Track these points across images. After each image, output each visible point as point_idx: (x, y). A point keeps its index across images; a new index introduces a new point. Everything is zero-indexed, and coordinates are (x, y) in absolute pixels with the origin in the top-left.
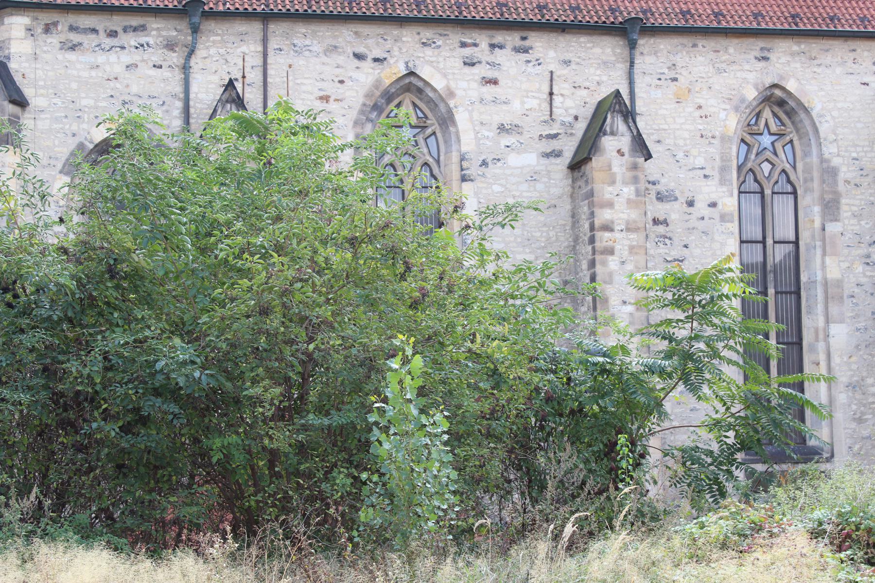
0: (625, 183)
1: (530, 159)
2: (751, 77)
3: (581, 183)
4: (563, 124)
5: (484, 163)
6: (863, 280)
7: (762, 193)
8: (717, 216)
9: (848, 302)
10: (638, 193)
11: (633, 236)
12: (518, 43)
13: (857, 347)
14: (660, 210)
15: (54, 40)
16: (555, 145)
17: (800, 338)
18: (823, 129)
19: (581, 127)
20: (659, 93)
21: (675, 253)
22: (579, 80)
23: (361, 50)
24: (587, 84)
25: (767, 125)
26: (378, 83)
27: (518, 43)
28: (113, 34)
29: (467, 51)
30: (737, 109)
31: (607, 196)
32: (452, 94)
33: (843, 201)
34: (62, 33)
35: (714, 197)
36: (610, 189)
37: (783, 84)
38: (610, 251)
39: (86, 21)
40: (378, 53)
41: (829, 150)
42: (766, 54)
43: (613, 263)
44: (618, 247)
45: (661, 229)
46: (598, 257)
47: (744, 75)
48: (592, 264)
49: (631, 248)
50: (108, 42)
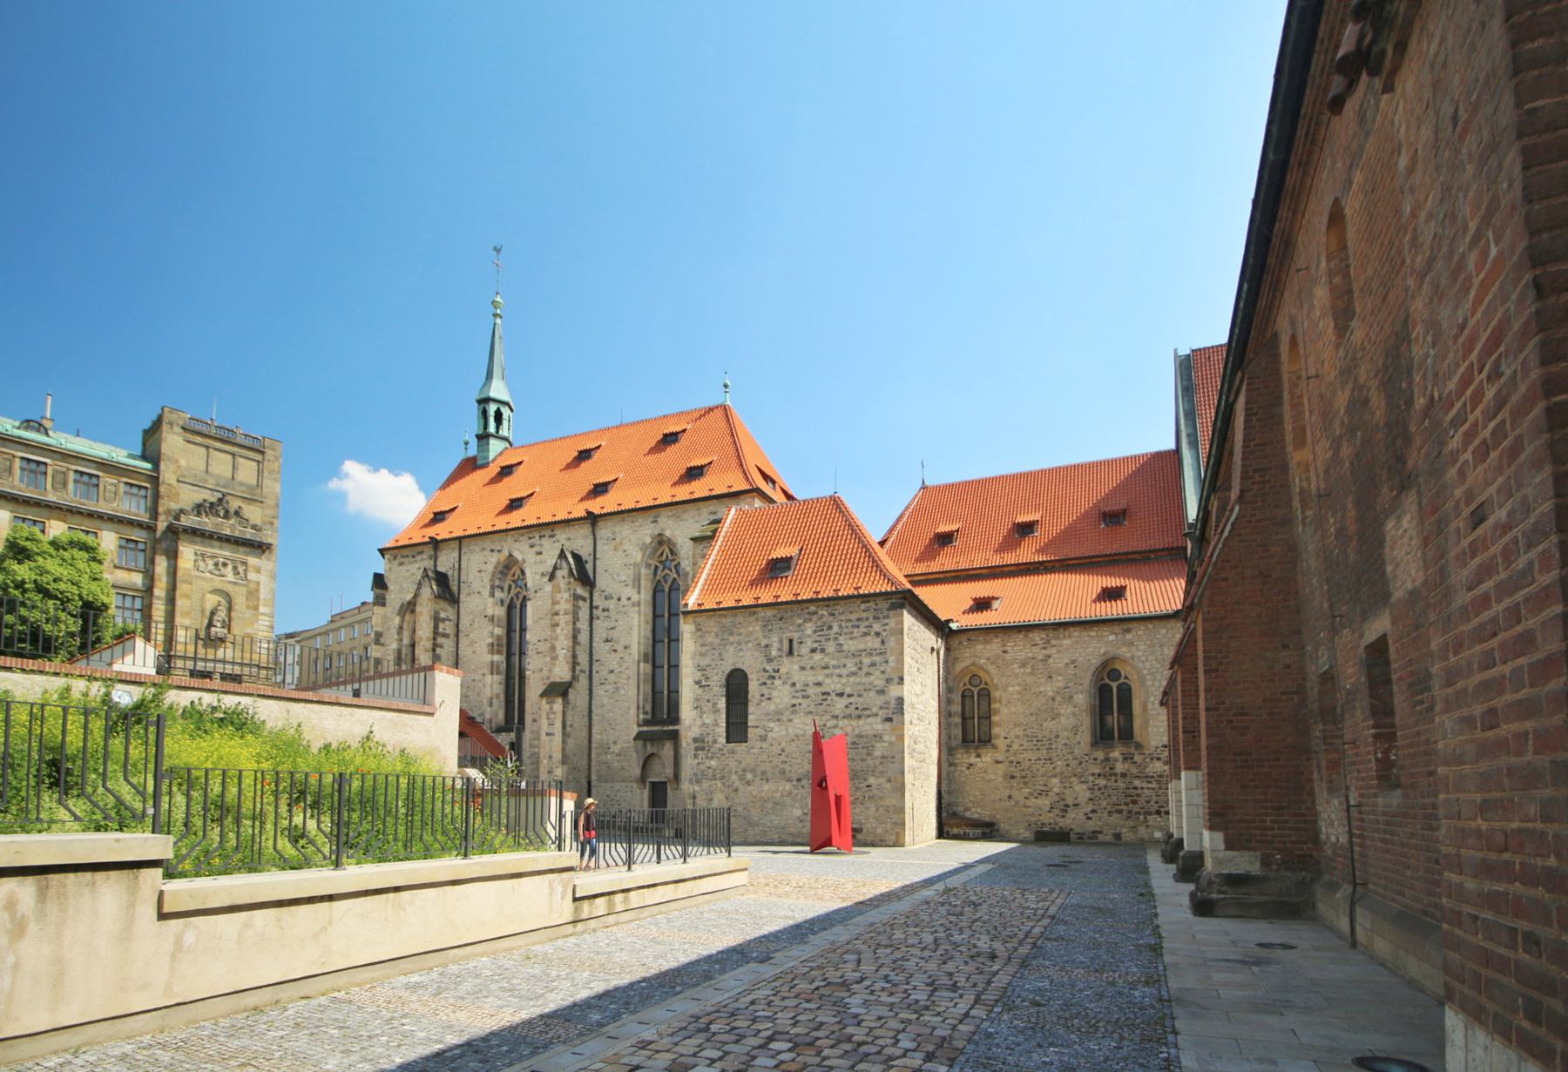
2: (649, 532)
5: (536, 591)
15: (396, 562)
21: (612, 625)
23: (493, 547)
26: (498, 562)
28: (414, 556)
30: (641, 549)
32: (524, 561)
34: (400, 560)
35: (629, 595)
38: (557, 625)
39: (405, 552)
40: (499, 548)
43: (558, 630)
45: (606, 614)
50: (412, 559)
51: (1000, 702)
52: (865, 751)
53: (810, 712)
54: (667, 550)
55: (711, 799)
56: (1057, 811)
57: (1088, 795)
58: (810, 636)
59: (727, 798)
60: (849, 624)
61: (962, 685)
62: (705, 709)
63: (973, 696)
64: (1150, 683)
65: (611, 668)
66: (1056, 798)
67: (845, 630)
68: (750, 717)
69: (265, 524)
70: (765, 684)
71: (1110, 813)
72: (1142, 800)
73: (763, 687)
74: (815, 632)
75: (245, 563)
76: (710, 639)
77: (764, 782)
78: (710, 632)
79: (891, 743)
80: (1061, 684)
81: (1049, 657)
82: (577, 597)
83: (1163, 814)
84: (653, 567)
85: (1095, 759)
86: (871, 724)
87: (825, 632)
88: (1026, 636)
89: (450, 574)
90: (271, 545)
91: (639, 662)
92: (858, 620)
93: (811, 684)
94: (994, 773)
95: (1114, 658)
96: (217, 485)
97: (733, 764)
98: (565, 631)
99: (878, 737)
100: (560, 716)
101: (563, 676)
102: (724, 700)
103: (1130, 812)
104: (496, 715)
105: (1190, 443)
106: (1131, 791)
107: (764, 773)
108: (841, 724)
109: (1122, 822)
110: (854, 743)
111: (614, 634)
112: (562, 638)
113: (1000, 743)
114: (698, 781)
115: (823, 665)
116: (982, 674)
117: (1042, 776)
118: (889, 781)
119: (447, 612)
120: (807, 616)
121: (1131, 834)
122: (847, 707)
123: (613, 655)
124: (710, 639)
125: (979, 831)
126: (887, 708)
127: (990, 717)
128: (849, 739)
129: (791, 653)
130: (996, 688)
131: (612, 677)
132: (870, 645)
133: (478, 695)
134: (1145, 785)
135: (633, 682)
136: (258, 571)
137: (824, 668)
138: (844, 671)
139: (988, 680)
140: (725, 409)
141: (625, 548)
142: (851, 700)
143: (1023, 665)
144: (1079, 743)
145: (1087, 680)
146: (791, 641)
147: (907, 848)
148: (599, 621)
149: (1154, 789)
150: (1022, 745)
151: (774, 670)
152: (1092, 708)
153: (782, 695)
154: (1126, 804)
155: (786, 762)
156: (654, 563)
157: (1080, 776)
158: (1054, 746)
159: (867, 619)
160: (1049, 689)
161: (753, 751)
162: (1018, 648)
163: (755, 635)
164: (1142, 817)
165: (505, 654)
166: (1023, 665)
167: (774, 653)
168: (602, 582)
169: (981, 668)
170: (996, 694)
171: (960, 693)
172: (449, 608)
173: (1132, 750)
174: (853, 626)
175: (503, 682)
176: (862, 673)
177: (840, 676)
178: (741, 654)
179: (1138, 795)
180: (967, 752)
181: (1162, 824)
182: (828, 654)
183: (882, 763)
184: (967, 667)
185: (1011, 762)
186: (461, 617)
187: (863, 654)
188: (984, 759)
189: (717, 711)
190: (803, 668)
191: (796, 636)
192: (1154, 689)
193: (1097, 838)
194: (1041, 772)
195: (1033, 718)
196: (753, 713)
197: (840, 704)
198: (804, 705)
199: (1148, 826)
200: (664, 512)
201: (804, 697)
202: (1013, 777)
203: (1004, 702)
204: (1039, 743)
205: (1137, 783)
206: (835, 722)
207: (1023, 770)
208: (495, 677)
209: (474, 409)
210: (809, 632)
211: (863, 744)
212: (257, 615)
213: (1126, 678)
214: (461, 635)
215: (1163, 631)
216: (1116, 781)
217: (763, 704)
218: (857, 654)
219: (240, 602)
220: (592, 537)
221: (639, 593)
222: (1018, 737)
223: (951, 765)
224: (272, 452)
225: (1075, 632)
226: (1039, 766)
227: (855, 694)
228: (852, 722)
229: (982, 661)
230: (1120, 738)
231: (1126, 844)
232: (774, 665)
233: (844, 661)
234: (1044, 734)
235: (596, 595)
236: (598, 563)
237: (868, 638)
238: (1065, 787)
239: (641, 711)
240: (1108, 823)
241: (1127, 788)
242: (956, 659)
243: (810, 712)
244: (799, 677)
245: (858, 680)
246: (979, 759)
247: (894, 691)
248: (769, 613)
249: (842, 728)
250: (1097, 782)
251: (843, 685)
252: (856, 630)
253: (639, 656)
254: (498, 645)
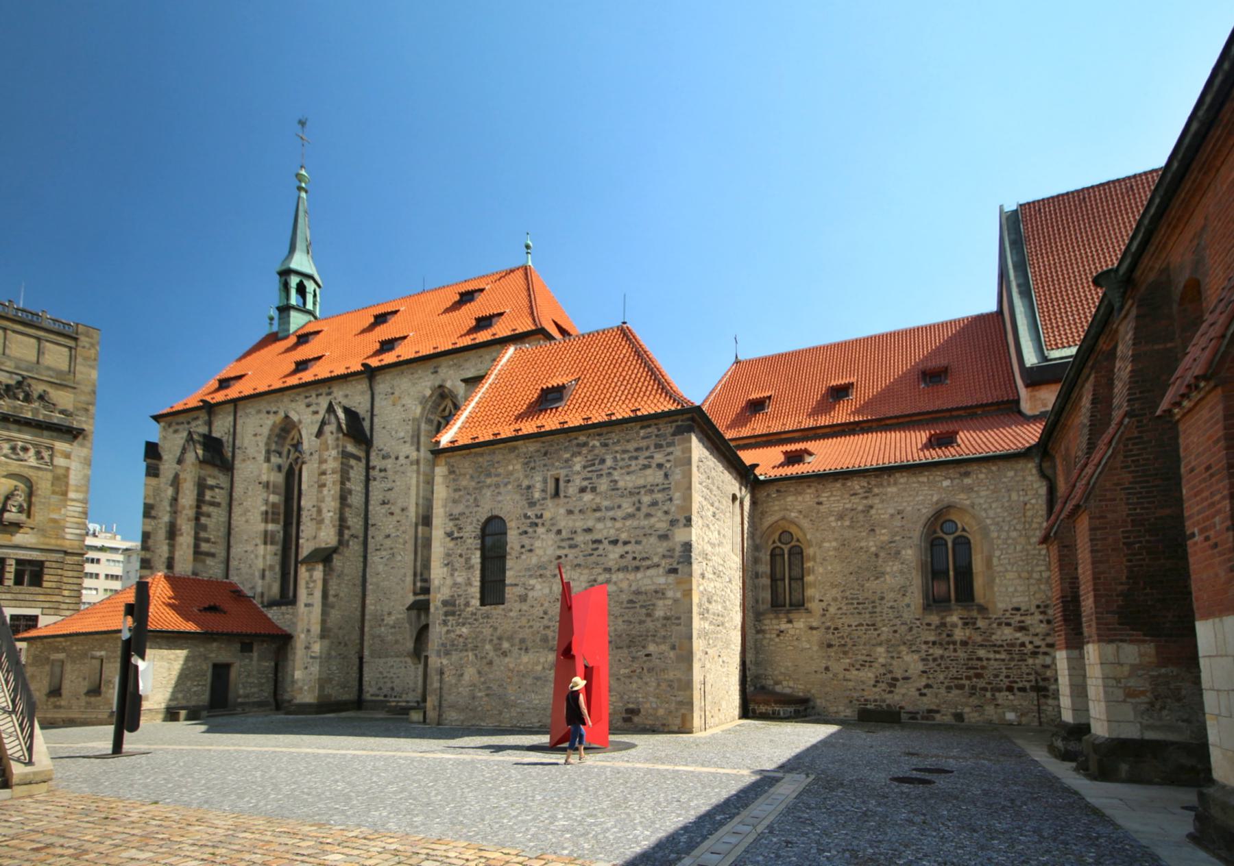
0: (333, 449)
2: (429, 384)
5: (311, 454)
11: (335, 476)
12: (327, 390)
20: (384, 403)
23: (269, 409)
26: (274, 425)
27: (327, 390)
29: (307, 400)
30: (421, 403)
32: (300, 422)
38: (324, 485)
40: (274, 409)
43: (325, 491)
51: (814, 559)
52: (644, 611)
53: (579, 565)
54: (450, 405)
55: (462, 675)
56: (884, 686)
57: (921, 667)
58: (578, 473)
59: (479, 673)
61: (770, 542)
62: (457, 565)
63: (783, 555)
64: (995, 535)
65: (387, 532)
66: (882, 671)
67: (621, 464)
68: (509, 574)
69: (78, 410)
70: (526, 532)
71: (949, 688)
72: (988, 674)
73: (524, 536)
74: (585, 467)
75: (51, 448)
76: (464, 482)
77: (523, 652)
78: (465, 475)
79: (676, 601)
80: (885, 538)
81: (871, 507)
82: (345, 455)
83: (1016, 690)
84: (435, 423)
85: (929, 624)
86: (651, 577)
87: (597, 467)
88: (843, 485)
89: (225, 439)
90: (84, 430)
91: (417, 525)
93: (579, 530)
94: (808, 641)
95: (949, 507)
96: (17, 367)
97: (487, 631)
98: (332, 492)
99: (660, 593)
100: (320, 584)
101: (329, 541)
102: (478, 554)
103: (974, 688)
104: (270, 587)
105: (1021, 293)
106: (975, 662)
107: (523, 641)
108: (614, 578)
109: (964, 700)
110: (631, 601)
112: (329, 499)
113: (814, 606)
114: (447, 653)
115: (594, 507)
116: (793, 529)
117: (865, 644)
118: (673, 648)
119: (215, 478)
120: (575, 449)
121: (976, 714)
122: (622, 556)
123: (390, 518)
124: (464, 482)
125: (791, 709)
126: (672, 557)
127: (802, 579)
128: (624, 597)
129: (557, 494)
130: (810, 544)
132: (650, 479)
133: (250, 567)
134: (992, 656)
135: (410, 546)
136: (67, 456)
137: (595, 510)
138: (619, 514)
139: (800, 535)
140: (526, 269)
141: (404, 402)
142: (628, 548)
143: (841, 517)
144: (908, 606)
145: (917, 532)
146: (557, 480)
147: (697, 735)
148: (375, 483)
149: (1003, 660)
150: (840, 609)
151: (536, 516)
152: (923, 565)
153: (545, 546)
154: (968, 678)
155: (548, 627)
156: (436, 418)
157: (910, 645)
158: (878, 610)
160: (871, 544)
161: (511, 614)
162: (835, 499)
163: (516, 475)
164: (989, 695)
165: (282, 523)
166: (841, 517)
167: (537, 495)
168: (380, 440)
169: (793, 522)
170: (810, 551)
171: (769, 553)
172: (220, 475)
173: (975, 614)
175: (279, 552)
176: (641, 514)
177: (614, 519)
178: (500, 498)
179: (983, 668)
180: (777, 618)
181: (1016, 703)
182: (600, 493)
183: (665, 625)
184: (776, 522)
185: (828, 628)
186: (236, 485)
187: (643, 491)
188: (796, 625)
189: (470, 567)
190: (570, 512)
191: (562, 473)
192: (1000, 542)
193: (934, 719)
194: (863, 640)
195: (853, 578)
196: (511, 569)
197: (614, 553)
198: (571, 557)
199: (997, 705)
200: (444, 361)
201: (571, 547)
202: (830, 646)
203: (818, 560)
204: (860, 606)
205: (982, 653)
206: (608, 576)
207: (842, 637)
208: (269, 547)
209: (276, 281)
210: (578, 468)
211: (641, 602)
212: (66, 500)
213: (964, 530)
214: (235, 503)
215: (1011, 474)
216: (955, 650)
217: (524, 557)
218: (634, 492)
219: (44, 485)
220: (369, 392)
221: (418, 450)
222: (835, 599)
223: (758, 632)
224: (87, 339)
225: (902, 479)
226: (860, 633)
227: (633, 541)
228: (628, 576)
229: (793, 515)
230: (957, 600)
231: (972, 729)
232: (537, 510)
233: (618, 501)
234: (866, 595)
235: (373, 455)
236: (376, 420)
238: (892, 657)
239: (419, 578)
240: (946, 700)
241: (968, 659)
242: (763, 513)
243: (579, 565)
244: (564, 523)
245: (636, 523)
246: (790, 626)
247: (679, 536)
248: (532, 447)
249: (615, 583)
250: (931, 651)
251: (617, 530)
253: (417, 517)
254: (273, 513)
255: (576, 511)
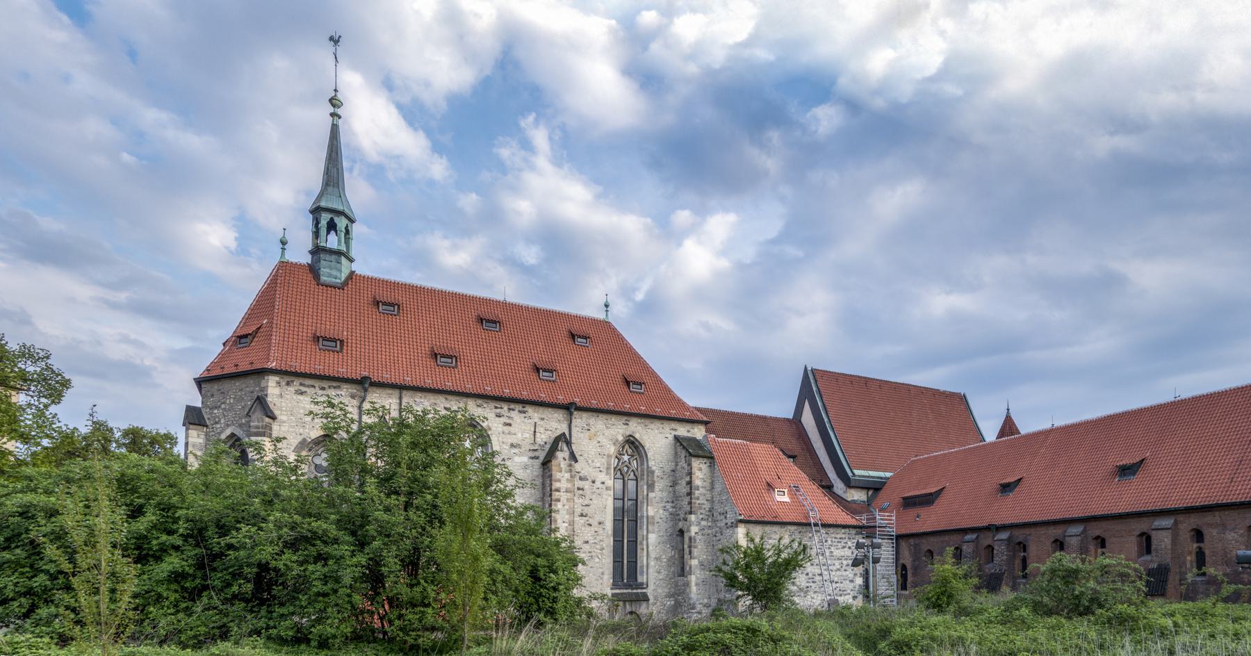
0: (566, 472)
1: (525, 459)
2: (621, 431)
3: (547, 471)
4: (540, 445)
6: (662, 516)
7: (623, 479)
8: (605, 488)
9: (656, 525)
10: (571, 476)
11: (569, 494)
13: (659, 543)
14: (579, 483)
16: (536, 454)
17: (637, 539)
18: (649, 455)
19: (548, 447)
21: (586, 502)
22: (548, 427)
24: (551, 429)
25: (627, 451)
30: (614, 444)
31: (558, 477)
33: (656, 484)
35: (603, 480)
36: (560, 474)
37: (634, 435)
41: (651, 463)
42: (628, 422)
43: (559, 505)
44: (562, 499)
45: (581, 492)
46: (553, 502)
47: (618, 430)
48: (550, 505)
49: (568, 499)
60: (836, 540)
92: (840, 538)
98: (567, 507)
111: (586, 510)
131: (586, 547)
132: (846, 553)
142: (837, 585)
159: (845, 538)
174: (838, 542)
176: (843, 569)
198: (813, 587)
201: (813, 582)
233: (834, 562)
237: (846, 549)
252: (839, 544)
255: (815, 564)
